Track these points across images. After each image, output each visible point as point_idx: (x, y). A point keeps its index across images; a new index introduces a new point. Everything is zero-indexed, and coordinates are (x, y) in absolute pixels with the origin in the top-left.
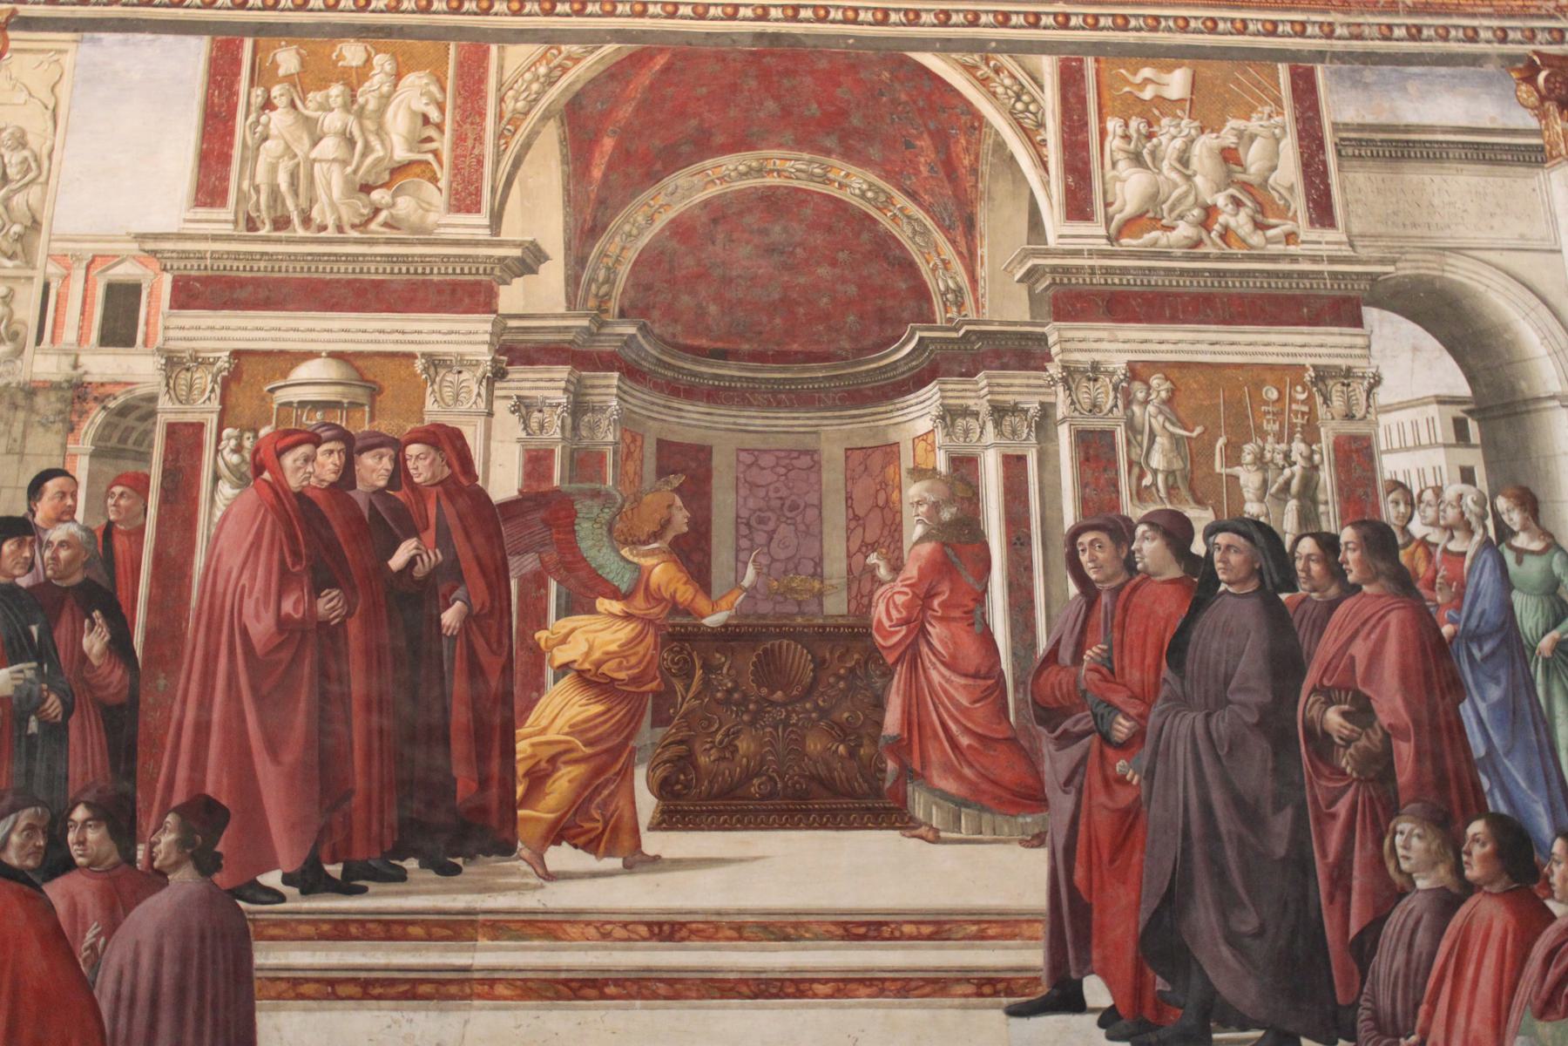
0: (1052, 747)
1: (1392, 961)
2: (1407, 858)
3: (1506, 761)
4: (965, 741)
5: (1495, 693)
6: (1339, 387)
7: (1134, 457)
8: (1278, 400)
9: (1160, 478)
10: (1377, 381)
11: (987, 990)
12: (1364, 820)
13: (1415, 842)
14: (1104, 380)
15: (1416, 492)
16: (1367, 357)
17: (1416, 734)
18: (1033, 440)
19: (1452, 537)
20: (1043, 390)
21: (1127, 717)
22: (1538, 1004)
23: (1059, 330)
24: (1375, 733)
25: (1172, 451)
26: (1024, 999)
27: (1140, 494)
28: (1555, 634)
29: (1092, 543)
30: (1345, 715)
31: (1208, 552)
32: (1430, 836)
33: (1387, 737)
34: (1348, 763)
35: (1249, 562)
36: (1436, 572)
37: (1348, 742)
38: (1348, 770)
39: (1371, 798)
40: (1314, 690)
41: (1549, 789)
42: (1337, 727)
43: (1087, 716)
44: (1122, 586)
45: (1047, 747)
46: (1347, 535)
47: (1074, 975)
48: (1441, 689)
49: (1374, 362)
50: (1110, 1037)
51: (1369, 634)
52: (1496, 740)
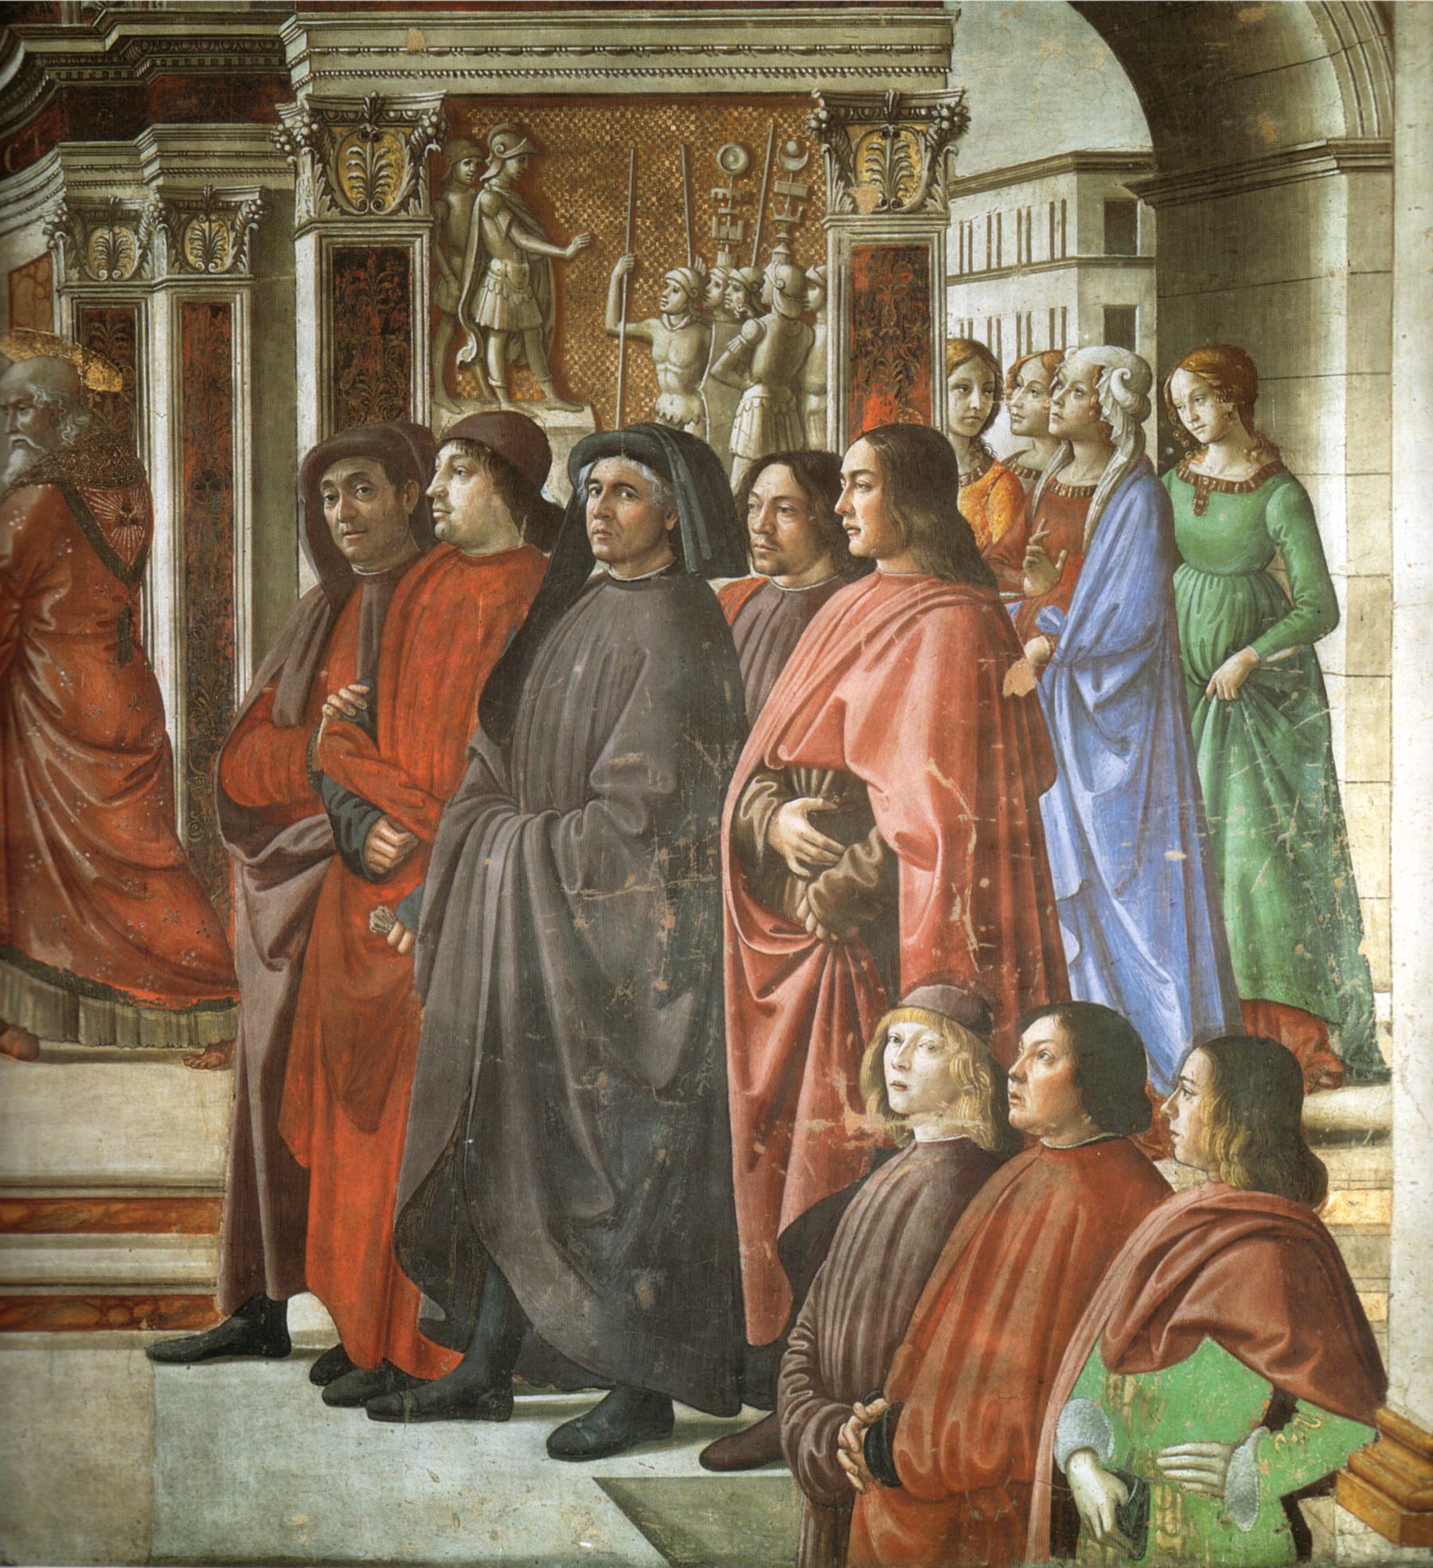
0: (251, 884)
1: (855, 1269)
2: (903, 1087)
3: (1115, 903)
4: (89, 869)
5: (1113, 768)
6: (876, 140)
7: (447, 305)
8: (746, 173)
9: (493, 343)
10: (958, 122)
11: (116, 1316)
12: (828, 1019)
13: (924, 1062)
14: (395, 147)
15: (1006, 366)
16: (942, 70)
17: (948, 855)
18: (244, 269)
19: (1070, 457)
20: (272, 163)
21: (395, 825)
22: (1115, 1342)
23: (308, 30)
24: (869, 854)
25: (520, 287)
26: (182, 1334)
27: (448, 385)
28: (1249, 653)
29: (349, 483)
30: (815, 818)
31: (575, 498)
32: (952, 1045)
33: (890, 857)
34: (809, 909)
35: (660, 514)
36: (1028, 528)
37: (816, 868)
38: (809, 923)
39: (846, 975)
40: (760, 769)
41: (1192, 957)
42: (795, 841)
43: (322, 823)
44: (405, 567)
45: (242, 883)
46: (858, 456)
47: (271, 1293)
48: (1009, 767)
49: (956, 82)
50: (331, 1401)
51: (879, 657)
52: (1103, 863)
